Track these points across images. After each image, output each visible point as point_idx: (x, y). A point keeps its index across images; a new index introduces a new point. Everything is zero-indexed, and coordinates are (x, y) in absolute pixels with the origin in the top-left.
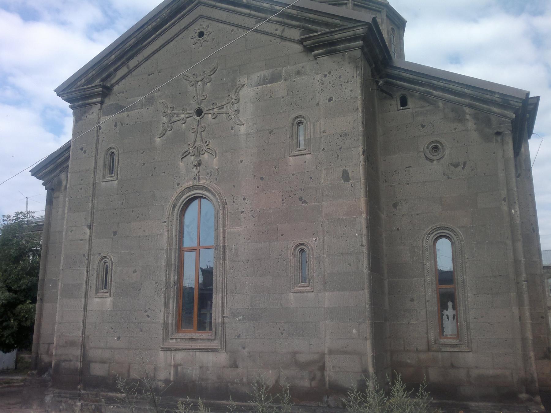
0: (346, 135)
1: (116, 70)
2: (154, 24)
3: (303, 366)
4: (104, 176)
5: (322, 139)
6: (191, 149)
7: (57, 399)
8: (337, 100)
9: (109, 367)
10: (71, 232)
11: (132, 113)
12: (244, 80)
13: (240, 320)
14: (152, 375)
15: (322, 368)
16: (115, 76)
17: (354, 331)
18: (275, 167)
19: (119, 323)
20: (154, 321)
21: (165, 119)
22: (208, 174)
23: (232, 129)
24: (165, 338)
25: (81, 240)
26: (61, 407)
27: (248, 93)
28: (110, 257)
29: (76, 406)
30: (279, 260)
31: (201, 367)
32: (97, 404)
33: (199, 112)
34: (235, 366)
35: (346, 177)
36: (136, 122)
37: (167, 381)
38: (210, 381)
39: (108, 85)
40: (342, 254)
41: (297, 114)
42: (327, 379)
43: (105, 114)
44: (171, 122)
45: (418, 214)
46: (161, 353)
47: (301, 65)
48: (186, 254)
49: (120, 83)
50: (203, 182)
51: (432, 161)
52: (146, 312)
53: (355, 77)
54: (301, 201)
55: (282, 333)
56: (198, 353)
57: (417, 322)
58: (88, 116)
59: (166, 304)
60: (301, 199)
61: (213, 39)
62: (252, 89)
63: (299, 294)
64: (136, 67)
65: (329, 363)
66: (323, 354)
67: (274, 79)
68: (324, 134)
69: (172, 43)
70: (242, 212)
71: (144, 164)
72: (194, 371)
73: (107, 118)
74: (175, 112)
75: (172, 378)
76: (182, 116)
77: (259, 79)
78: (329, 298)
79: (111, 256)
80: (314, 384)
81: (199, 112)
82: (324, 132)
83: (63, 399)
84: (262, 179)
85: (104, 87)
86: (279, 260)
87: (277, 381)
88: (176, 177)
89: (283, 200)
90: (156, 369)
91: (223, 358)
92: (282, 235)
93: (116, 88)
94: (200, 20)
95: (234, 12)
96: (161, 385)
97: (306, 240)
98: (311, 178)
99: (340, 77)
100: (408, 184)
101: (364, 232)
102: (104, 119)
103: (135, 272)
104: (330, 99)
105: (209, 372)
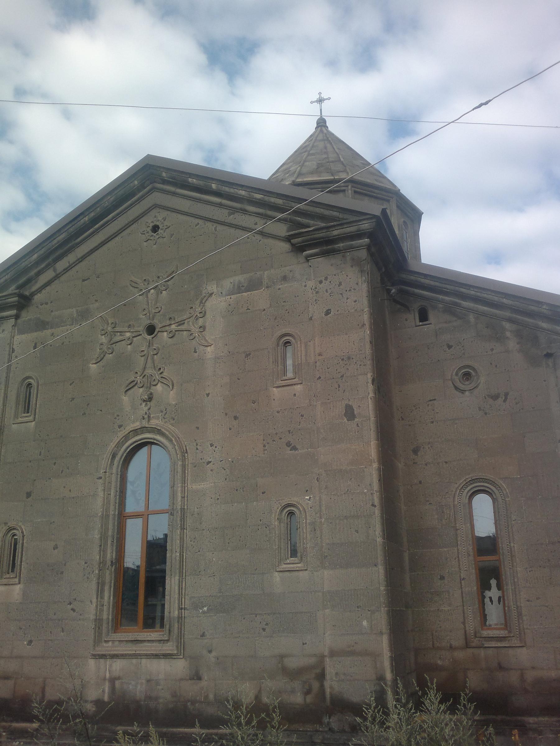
0: (349, 358)
1: (39, 274)
4: (16, 416)
5: (318, 364)
6: (139, 379)
8: (337, 313)
12: (212, 287)
13: (204, 612)
15: (321, 677)
16: (36, 282)
18: (254, 402)
20: (81, 617)
21: (104, 339)
22: (162, 412)
23: (195, 352)
24: (98, 640)
27: (217, 304)
28: (20, 527)
30: (260, 528)
31: (148, 681)
33: (151, 330)
34: (197, 677)
35: (350, 413)
37: (99, 703)
38: (161, 701)
39: (27, 293)
40: (346, 517)
41: (284, 331)
42: (328, 691)
43: (21, 332)
44: (112, 342)
45: (446, 462)
46: (92, 663)
47: (288, 268)
48: (130, 523)
49: (43, 291)
50: (154, 423)
51: (463, 392)
52: (70, 604)
53: (360, 284)
54: (289, 446)
55: (264, 630)
56: (144, 661)
57: (449, 608)
59: (100, 592)
60: (288, 444)
61: (172, 235)
62: (222, 298)
63: (287, 574)
64: (66, 270)
65: (331, 668)
66: (323, 657)
68: (320, 357)
69: (117, 238)
70: (209, 462)
71: (73, 399)
72: (139, 687)
73: (23, 336)
74: (117, 329)
75: (106, 699)
76: (128, 334)
77: (231, 287)
78: (329, 579)
79: (23, 527)
80: (309, 699)
81: (151, 330)
82: (320, 355)
84: (236, 418)
85: (21, 296)
86: (260, 528)
87: (257, 697)
88: (118, 416)
89: (264, 446)
90: (83, 686)
91: (179, 667)
92: (263, 493)
93: (38, 298)
94: (154, 211)
96: (90, 708)
97: (296, 499)
98: (302, 416)
99: (340, 284)
100: (432, 422)
101: (376, 486)
102: (18, 338)
103: (55, 548)
104: (328, 313)
105: (160, 687)
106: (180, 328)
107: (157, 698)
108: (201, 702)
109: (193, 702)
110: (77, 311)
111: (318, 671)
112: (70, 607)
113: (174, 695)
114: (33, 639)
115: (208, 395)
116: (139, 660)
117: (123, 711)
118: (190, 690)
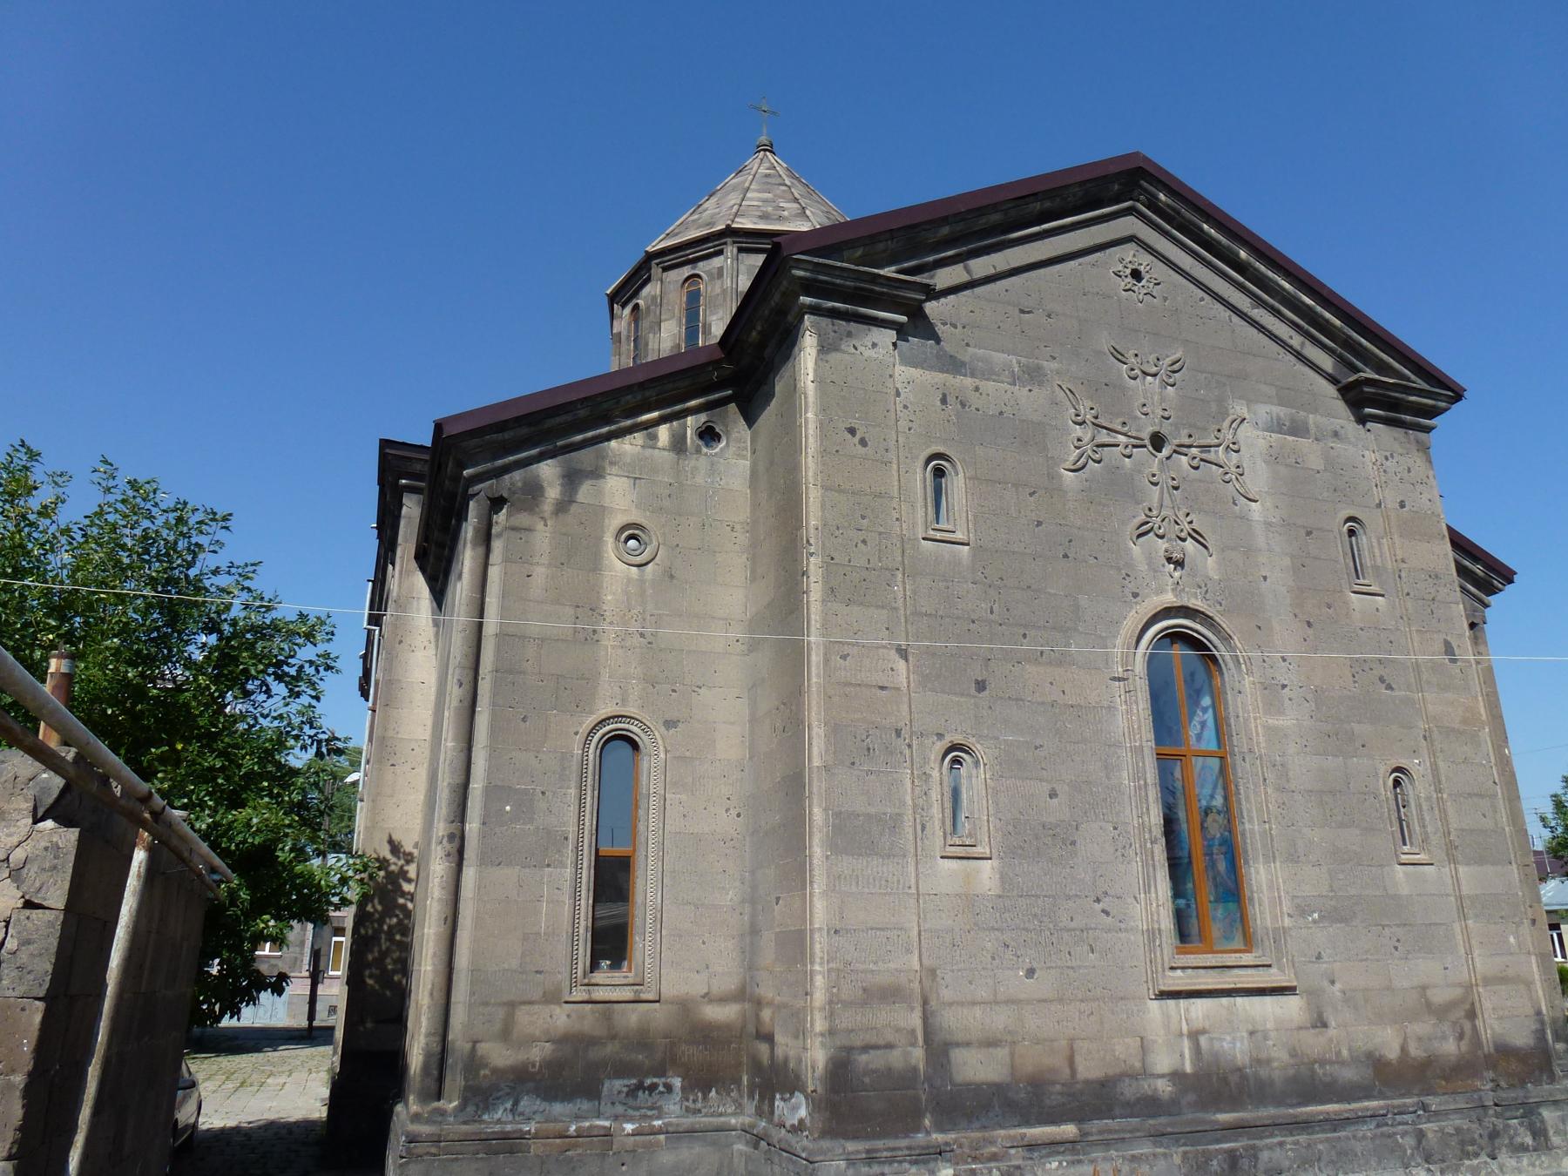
2: (1048, 204)
3: (1441, 1012)
7: (865, 1170)
9: (1012, 1055)
10: (844, 657)
11: (989, 386)
12: (1240, 409)
13: (1314, 921)
14: (1138, 1065)
15: (1472, 1015)
17: (1512, 939)
19: (1026, 930)
20: (1123, 926)
21: (1085, 433)
25: (882, 688)
31: (1252, 1033)
32: (1003, 1165)
34: (1321, 1023)
36: (1001, 413)
37: (1176, 1076)
38: (1275, 1064)
49: (943, 300)
52: (1098, 900)
56: (1239, 1000)
58: (861, 349)
60: (1382, 680)
61: (1165, 299)
65: (1488, 1002)
67: (1298, 430)
70: (1284, 686)
71: (1039, 524)
75: (1188, 1069)
76: (1121, 438)
81: (1158, 441)
84: (1309, 624)
87: (1403, 1049)
90: (1144, 1048)
91: (1291, 1008)
95: (1208, 264)
96: (1164, 1088)
103: (1053, 795)
105: (1270, 1043)
106: (1204, 456)
107: (1269, 1061)
108: (1331, 1063)
109: (1323, 1063)
111: (1467, 1006)
112: (1099, 907)
113: (1293, 1053)
114: (1035, 965)
115: (1265, 578)
116: (1231, 999)
117: (1215, 1085)
118: (1314, 1043)
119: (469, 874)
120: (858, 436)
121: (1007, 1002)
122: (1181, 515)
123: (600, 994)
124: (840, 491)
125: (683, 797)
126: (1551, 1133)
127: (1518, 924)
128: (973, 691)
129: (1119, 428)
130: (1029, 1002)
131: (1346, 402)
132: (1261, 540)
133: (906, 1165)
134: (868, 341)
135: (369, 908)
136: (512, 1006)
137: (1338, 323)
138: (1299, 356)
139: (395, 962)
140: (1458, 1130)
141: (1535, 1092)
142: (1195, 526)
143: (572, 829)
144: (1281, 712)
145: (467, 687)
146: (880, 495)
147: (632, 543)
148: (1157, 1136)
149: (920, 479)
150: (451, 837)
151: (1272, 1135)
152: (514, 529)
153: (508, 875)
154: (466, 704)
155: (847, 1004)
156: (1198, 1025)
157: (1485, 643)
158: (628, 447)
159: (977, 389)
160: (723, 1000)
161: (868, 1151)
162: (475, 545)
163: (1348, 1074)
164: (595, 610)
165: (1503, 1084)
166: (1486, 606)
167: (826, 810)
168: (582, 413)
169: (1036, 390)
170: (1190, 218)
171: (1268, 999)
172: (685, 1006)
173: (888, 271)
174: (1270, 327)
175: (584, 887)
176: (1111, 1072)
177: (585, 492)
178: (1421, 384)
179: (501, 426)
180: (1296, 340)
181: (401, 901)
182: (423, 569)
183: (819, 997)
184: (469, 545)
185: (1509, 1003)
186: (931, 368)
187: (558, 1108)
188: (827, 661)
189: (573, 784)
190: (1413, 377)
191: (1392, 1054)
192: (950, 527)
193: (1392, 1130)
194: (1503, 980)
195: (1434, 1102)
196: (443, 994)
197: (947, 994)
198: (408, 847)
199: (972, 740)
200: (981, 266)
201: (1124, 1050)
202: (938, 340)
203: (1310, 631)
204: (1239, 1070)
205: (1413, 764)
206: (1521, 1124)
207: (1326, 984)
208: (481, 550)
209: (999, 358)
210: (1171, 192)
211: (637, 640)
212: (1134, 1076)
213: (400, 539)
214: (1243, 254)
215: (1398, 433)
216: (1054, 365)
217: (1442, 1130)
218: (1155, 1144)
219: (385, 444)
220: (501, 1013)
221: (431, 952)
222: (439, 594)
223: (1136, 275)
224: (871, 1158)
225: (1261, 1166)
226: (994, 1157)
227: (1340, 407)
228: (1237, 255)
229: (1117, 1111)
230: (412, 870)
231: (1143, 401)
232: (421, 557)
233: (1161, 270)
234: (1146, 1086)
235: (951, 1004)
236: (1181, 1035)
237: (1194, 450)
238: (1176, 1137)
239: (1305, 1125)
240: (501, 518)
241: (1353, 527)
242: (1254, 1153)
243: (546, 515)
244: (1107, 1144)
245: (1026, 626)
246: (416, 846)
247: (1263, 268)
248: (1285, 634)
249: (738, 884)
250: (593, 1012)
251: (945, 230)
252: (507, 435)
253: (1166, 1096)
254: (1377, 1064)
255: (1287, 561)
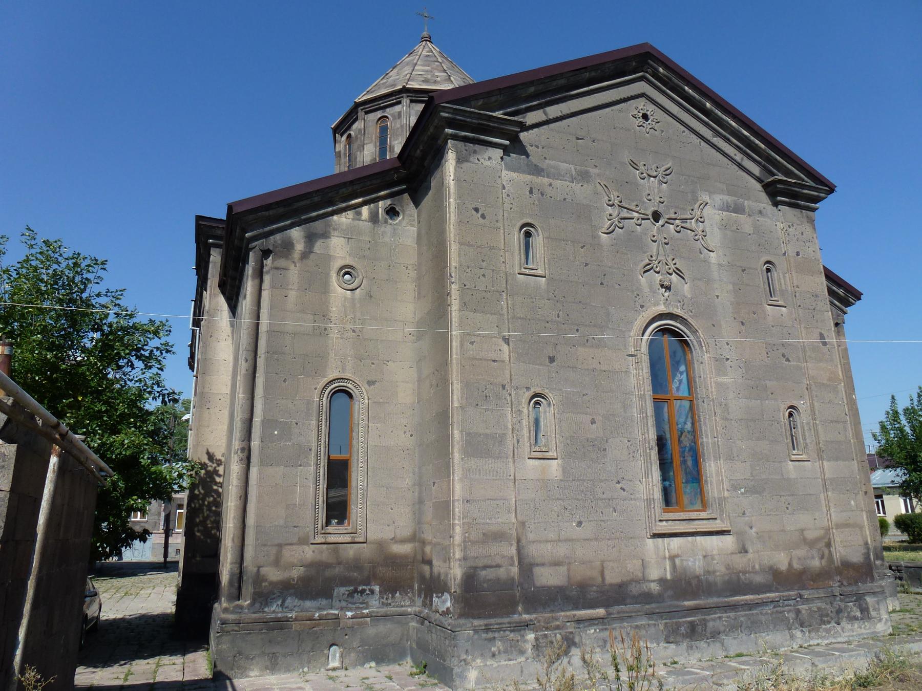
0: (817, 296)
2: (593, 74)
3: (811, 544)
7: (484, 635)
9: (569, 570)
10: (472, 343)
11: (557, 183)
12: (705, 197)
13: (742, 494)
14: (640, 575)
15: (829, 545)
17: (853, 503)
19: (578, 499)
21: (615, 211)
25: (494, 361)
26: (494, 649)
29: (526, 641)
31: (705, 557)
32: (563, 632)
36: (565, 199)
37: (662, 581)
40: (832, 422)
46: (650, 542)
49: (530, 131)
52: (619, 482)
56: (698, 538)
58: (482, 160)
60: (784, 356)
61: (662, 131)
65: (838, 538)
70: (727, 359)
71: (587, 265)
75: (669, 577)
76: (635, 214)
81: (656, 216)
83: (496, 635)
84: (743, 323)
87: (790, 564)
90: (644, 565)
91: (728, 542)
95: (688, 111)
96: (655, 588)
103: (593, 422)
106: (684, 225)
107: (714, 572)
108: (749, 572)
109: (744, 573)
110: (575, 169)
111: (826, 540)
112: (619, 486)
113: (728, 567)
114: (582, 519)
115: (718, 297)
118: (740, 562)
119: (254, 471)
120: (480, 213)
121: (567, 540)
122: (669, 259)
123: (332, 539)
124: (469, 245)
125: (379, 425)
126: (871, 609)
127: (856, 494)
128: (547, 362)
129: (634, 208)
130: (578, 540)
131: (767, 193)
132: (715, 274)
133: (508, 633)
134: (486, 156)
135: (196, 492)
136: (280, 546)
137: (763, 146)
138: (740, 166)
139: (212, 522)
140: (819, 609)
141: (862, 587)
142: (677, 266)
143: (314, 445)
144: (725, 374)
145: (251, 362)
146: (492, 248)
147: (347, 277)
148: (650, 614)
149: (516, 238)
150: (243, 450)
151: (715, 613)
152: (277, 268)
153: (276, 472)
154: (250, 372)
155: (474, 543)
156: (674, 552)
157: (844, 335)
158: (344, 220)
159: (550, 185)
160: (403, 541)
161: (486, 625)
162: (253, 278)
163: (759, 579)
164: (326, 316)
165: (845, 583)
166: (845, 313)
167: (461, 431)
168: (316, 199)
169: (585, 186)
170: (677, 83)
171: (714, 537)
172: (381, 545)
173: (498, 114)
174: (723, 149)
175: (321, 478)
176: (625, 579)
177: (318, 246)
178: (811, 183)
179: (268, 207)
180: (738, 157)
181: (215, 487)
182: (223, 293)
183: (458, 539)
184: (250, 278)
185: (850, 538)
186: (524, 172)
187: (308, 604)
188: (462, 345)
189: (314, 418)
190: (806, 179)
191: (784, 567)
192: (534, 267)
193: (782, 609)
194: (847, 525)
195: (806, 594)
196: (240, 540)
197: (531, 536)
198: (218, 456)
199: (547, 391)
200: (554, 111)
201: (633, 566)
202: (528, 156)
203: (743, 328)
204: (698, 577)
205: (801, 404)
206: (854, 605)
207: (747, 528)
208: (257, 281)
209: (564, 166)
210: (666, 67)
211: (351, 334)
212: (637, 581)
213: (209, 276)
214: (708, 105)
215: (796, 212)
216: (596, 171)
217: (810, 609)
218: (649, 619)
219: (199, 218)
220: (274, 550)
221: (232, 516)
222: (233, 308)
223: (645, 117)
224: (487, 629)
225: (708, 630)
226: (558, 627)
227: (763, 196)
228: (705, 105)
229: (628, 601)
230: (221, 470)
231: (648, 192)
232: (222, 286)
233: (660, 115)
234: (644, 587)
235: (534, 542)
236: (665, 558)
237: (678, 222)
238: (661, 615)
239: (734, 607)
240: (269, 262)
241: (769, 267)
242: (704, 623)
243: (296, 260)
244: (622, 619)
245: (578, 325)
246: (223, 455)
247: (720, 113)
248: (729, 331)
249: (411, 475)
250: (328, 549)
251: (532, 89)
252: (271, 212)
253: (656, 592)
254: (775, 573)
255: (730, 287)
